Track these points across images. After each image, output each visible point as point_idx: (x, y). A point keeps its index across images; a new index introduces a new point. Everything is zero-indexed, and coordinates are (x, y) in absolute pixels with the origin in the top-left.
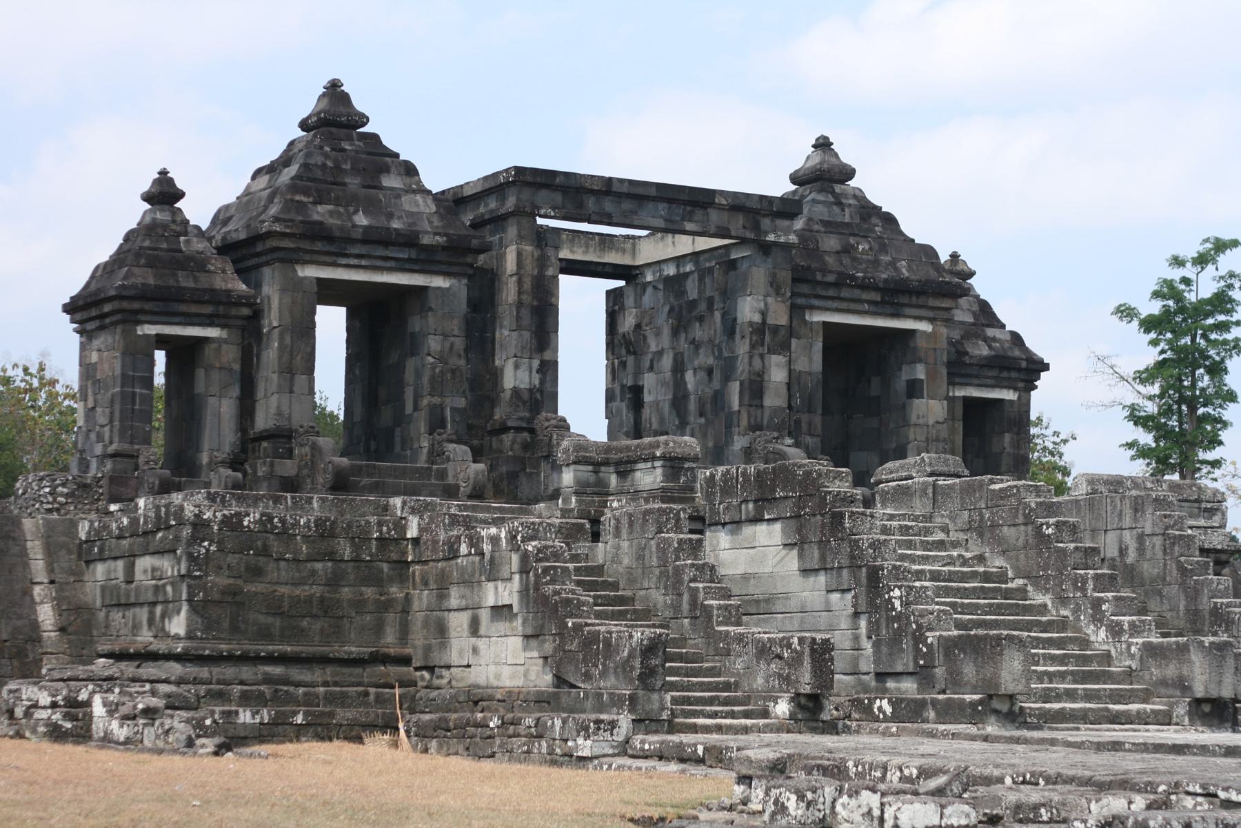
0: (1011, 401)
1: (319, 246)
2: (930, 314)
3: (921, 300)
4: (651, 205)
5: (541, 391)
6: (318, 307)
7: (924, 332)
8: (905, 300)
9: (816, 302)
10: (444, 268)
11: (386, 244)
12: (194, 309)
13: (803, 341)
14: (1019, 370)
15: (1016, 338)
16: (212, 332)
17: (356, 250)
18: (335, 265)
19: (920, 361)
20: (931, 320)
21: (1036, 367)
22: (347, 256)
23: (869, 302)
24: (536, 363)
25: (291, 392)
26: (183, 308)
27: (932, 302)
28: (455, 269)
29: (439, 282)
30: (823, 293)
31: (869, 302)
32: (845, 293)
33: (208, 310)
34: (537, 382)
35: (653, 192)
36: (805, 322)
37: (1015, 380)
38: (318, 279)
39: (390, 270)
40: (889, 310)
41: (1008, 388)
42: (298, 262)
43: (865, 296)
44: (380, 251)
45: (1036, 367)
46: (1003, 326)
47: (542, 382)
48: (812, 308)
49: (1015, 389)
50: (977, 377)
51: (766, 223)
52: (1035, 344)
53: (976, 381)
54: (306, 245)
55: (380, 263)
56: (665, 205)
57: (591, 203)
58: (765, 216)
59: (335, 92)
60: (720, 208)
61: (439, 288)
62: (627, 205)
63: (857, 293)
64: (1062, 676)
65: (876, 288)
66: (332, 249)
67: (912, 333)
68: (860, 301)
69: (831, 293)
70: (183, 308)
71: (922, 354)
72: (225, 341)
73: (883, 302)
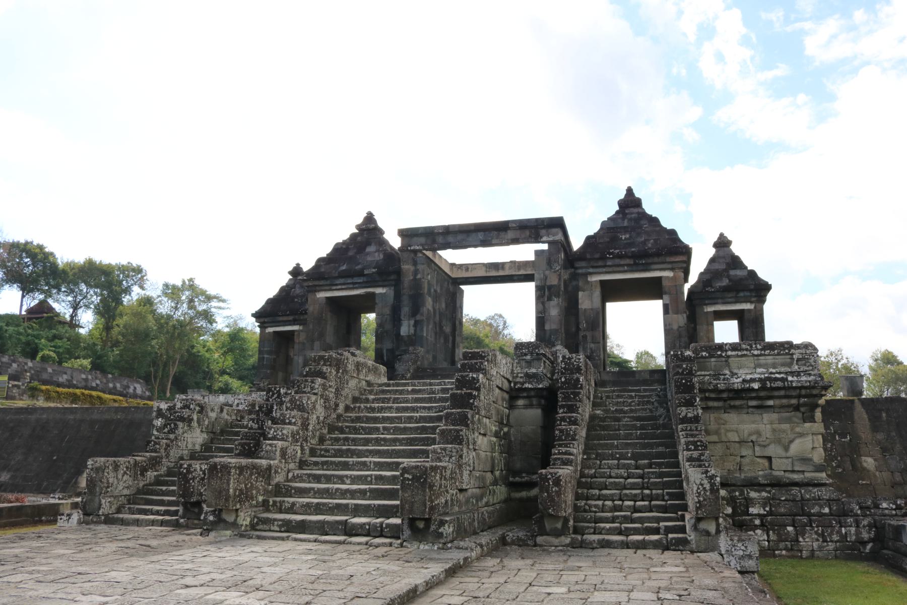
0: (749, 310)
1: (322, 283)
2: (670, 266)
3: (661, 259)
4: (474, 235)
5: (415, 335)
6: (716, 323)
7: (668, 277)
8: (650, 261)
9: (591, 270)
10: (381, 283)
11: (352, 276)
12: (285, 318)
13: (586, 293)
14: (751, 291)
15: (753, 274)
16: (296, 328)
17: (338, 282)
18: (331, 290)
19: (666, 293)
20: (672, 269)
21: (766, 287)
22: (337, 285)
23: (628, 265)
24: (412, 322)
25: (312, 349)
26: (281, 319)
27: (668, 259)
28: (386, 283)
29: (379, 291)
30: (596, 264)
31: (628, 265)
32: (609, 263)
33: (291, 318)
34: (412, 331)
35: (473, 228)
36: (588, 282)
37: (751, 296)
38: (327, 298)
39: (357, 288)
40: (641, 267)
41: (746, 302)
42: (316, 291)
43: (622, 262)
44: (349, 281)
45: (766, 287)
46: (746, 268)
47: (415, 331)
48: (591, 274)
49: (751, 302)
50: (722, 298)
51: (543, 232)
52: (762, 275)
53: (720, 301)
54: (317, 283)
55: (351, 286)
56: (482, 233)
57: (440, 240)
58: (542, 229)
59: (370, 218)
60: (514, 229)
61: (380, 294)
62: (460, 237)
63: (617, 261)
64: (363, 494)
65: (630, 257)
66: (328, 282)
67: (660, 278)
68: (623, 265)
69: (600, 263)
70: (281, 319)
71: (667, 289)
72: (302, 331)
73: (635, 264)
